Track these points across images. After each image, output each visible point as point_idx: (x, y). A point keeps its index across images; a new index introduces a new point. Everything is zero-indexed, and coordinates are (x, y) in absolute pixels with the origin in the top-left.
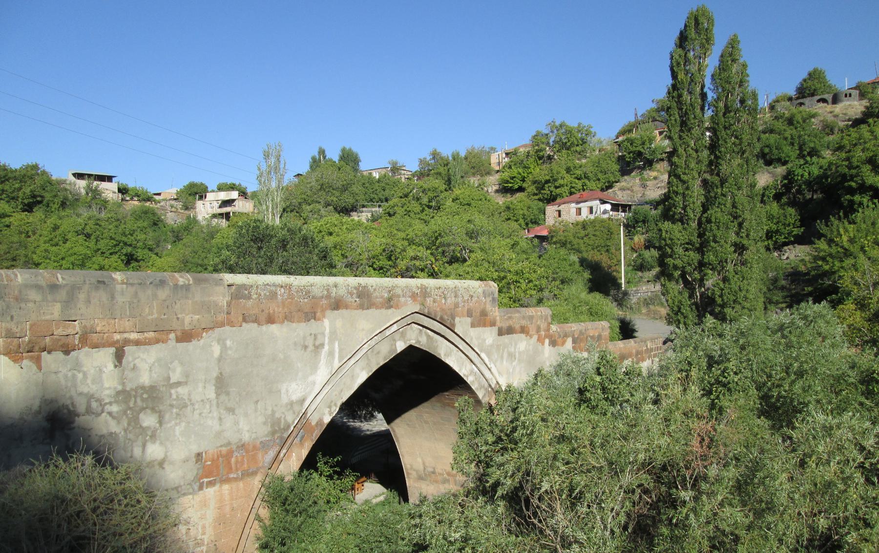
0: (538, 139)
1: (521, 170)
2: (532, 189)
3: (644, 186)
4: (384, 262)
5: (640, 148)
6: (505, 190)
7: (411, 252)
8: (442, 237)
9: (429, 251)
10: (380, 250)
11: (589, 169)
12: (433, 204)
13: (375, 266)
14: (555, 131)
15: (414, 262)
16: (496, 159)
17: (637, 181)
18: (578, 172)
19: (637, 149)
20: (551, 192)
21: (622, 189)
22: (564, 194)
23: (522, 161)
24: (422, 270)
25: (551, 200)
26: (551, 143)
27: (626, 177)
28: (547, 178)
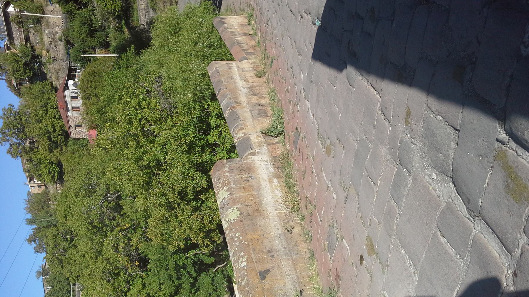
0: (14, 153)
1: (43, 166)
2: (56, 152)
3: (55, 59)
4: (121, 281)
5: (21, 64)
6: (60, 179)
7: (109, 253)
8: (93, 221)
9: (109, 234)
10: (108, 286)
11: (38, 103)
12: (69, 237)
13: (126, 289)
14: (7, 138)
15: (120, 249)
16: (35, 188)
17: (51, 66)
18: (41, 112)
19: (22, 66)
20: (59, 135)
21: (58, 78)
22: (61, 124)
23: (35, 165)
24: (129, 239)
25: (67, 135)
26: (18, 141)
27: (48, 77)
28: (46, 138)
